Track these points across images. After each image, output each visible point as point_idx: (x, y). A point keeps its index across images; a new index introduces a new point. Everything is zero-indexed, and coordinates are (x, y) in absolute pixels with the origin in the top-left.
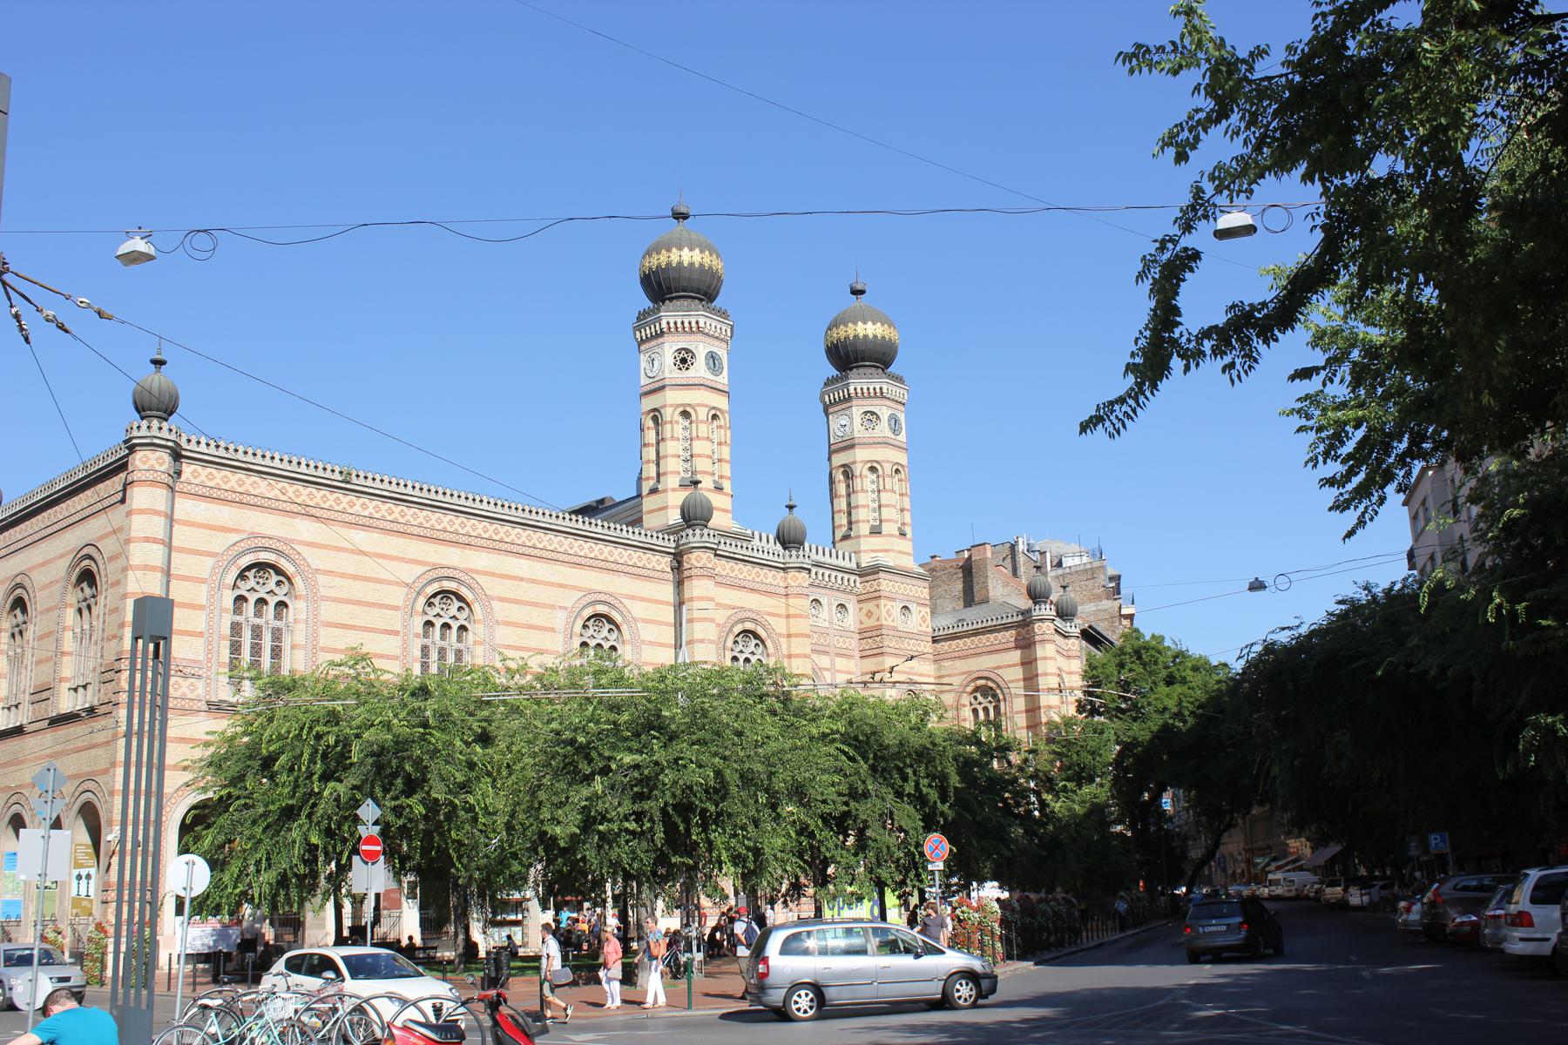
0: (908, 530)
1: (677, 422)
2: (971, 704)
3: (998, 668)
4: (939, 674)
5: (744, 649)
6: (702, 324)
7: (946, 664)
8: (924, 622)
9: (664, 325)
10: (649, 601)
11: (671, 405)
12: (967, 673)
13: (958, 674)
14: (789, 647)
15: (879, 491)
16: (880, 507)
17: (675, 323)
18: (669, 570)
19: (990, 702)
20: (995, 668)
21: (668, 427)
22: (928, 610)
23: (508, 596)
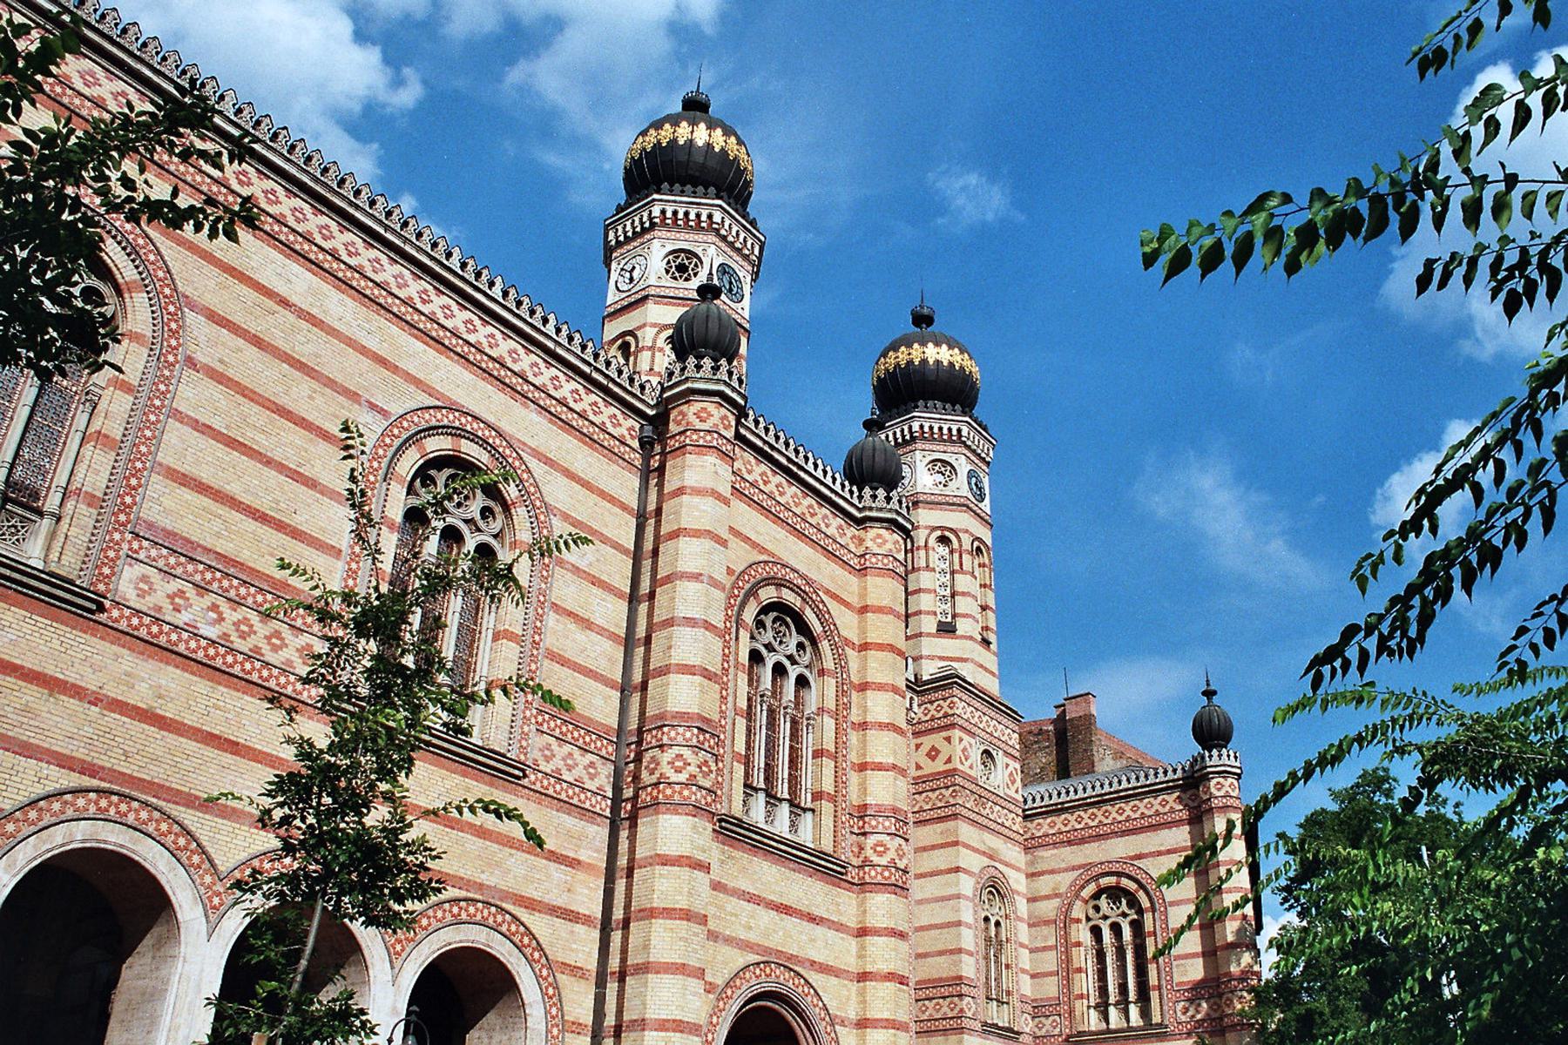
0: (992, 637)
1: (661, 350)
2: (1088, 919)
3: (1140, 857)
4: (1030, 871)
5: (776, 645)
6: (717, 217)
7: (1042, 853)
8: (1013, 782)
9: (656, 211)
10: (586, 485)
11: (654, 325)
12: (1080, 867)
13: (1066, 870)
14: (863, 668)
15: (953, 573)
16: (953, 596)
17: (675, 213)
18: (636, 444)
19: (1124, 915)
20: (1132, 858)
21: (645, 356)
22: (1018, 766)
23: (237, 319)
